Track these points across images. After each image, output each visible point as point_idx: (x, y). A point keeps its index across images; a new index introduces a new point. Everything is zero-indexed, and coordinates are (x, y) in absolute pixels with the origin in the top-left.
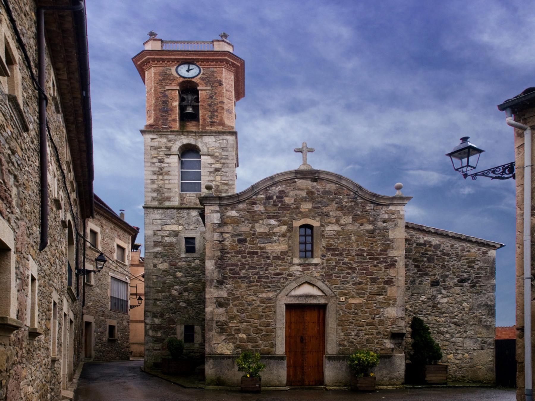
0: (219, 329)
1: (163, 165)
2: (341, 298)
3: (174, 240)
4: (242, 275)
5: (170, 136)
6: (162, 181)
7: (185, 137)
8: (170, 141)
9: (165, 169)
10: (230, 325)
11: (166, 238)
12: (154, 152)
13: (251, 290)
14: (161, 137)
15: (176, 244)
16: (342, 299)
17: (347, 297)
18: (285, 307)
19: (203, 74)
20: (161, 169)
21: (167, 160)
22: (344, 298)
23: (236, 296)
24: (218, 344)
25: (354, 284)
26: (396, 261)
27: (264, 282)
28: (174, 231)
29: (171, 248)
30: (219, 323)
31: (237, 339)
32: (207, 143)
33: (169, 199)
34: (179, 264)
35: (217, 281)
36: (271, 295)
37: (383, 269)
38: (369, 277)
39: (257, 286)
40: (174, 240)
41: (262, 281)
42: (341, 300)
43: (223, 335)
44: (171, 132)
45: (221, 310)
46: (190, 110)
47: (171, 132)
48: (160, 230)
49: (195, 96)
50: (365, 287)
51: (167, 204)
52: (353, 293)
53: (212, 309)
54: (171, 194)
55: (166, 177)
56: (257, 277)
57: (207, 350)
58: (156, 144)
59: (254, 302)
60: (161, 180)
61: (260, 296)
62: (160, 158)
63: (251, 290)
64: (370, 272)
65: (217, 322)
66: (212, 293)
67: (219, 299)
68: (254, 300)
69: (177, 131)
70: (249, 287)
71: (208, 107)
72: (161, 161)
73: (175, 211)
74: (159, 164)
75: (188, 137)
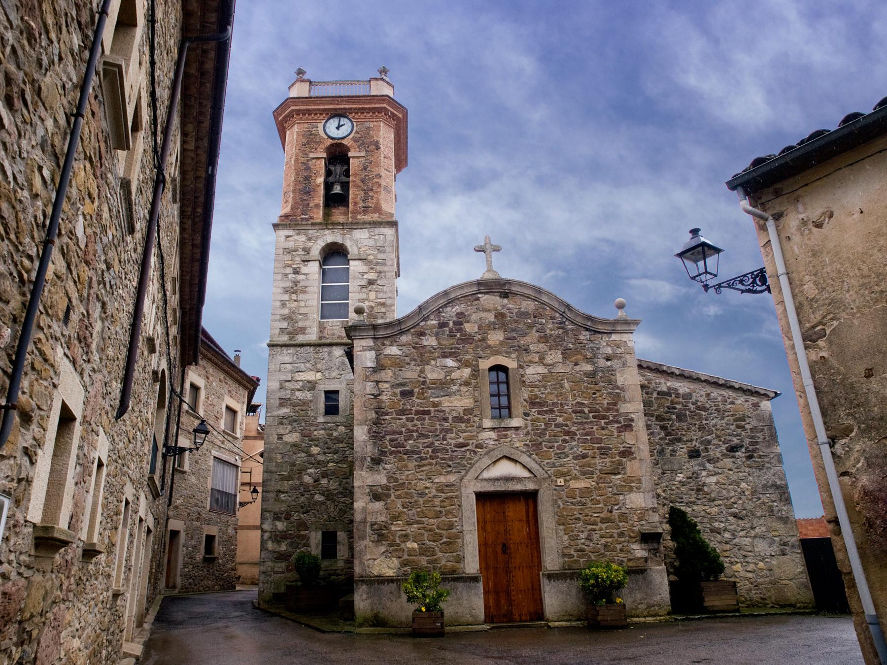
0: (376, 536)
2: (559, 480)
3: (308, 395)
11: (298, 393)
15: (311, 401)
16: (560, 481)
17: (568, 478)
22: (562, 480)
23: (400, 481)
25: (575, 458)
26: (632, 420)
28: (309, 382)
29: (304, 408)
37: (616, 433)
38: (596, 445)
40: (308, 395)
42: (559, 484)
43: (382, 545)
45: (379, 505)
52: (575, 472)
59: (427, 491)
61: (437, 480)
64: (597, 438)
66: (363, 479)
67: (374, 488)
68: (427, 488)
70: (419, 466)
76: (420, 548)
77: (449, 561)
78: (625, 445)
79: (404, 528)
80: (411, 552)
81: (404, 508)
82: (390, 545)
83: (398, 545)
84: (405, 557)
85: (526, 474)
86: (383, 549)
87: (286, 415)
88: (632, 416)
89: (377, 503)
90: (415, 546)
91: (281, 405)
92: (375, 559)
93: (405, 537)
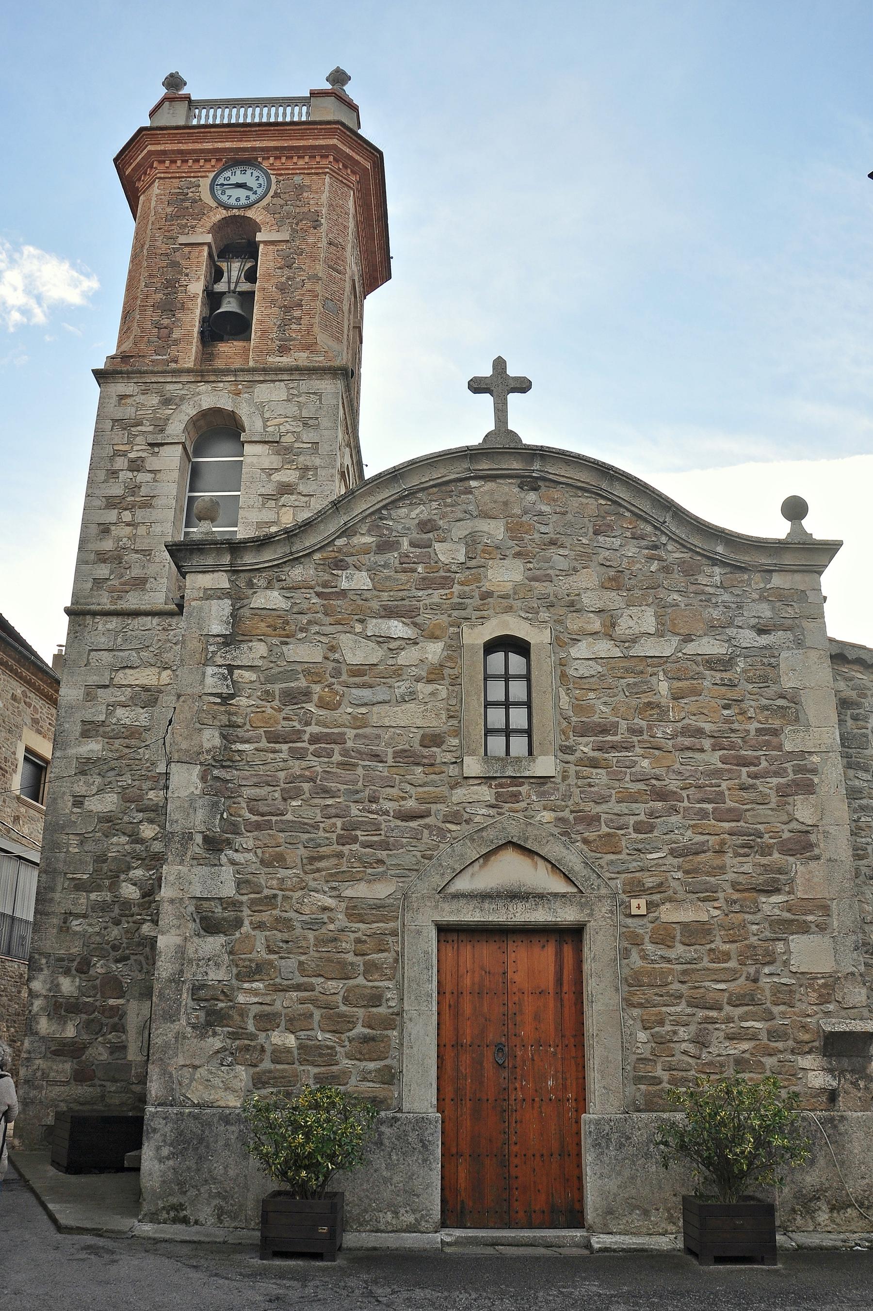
0: (202, 1014)
1: (141, 477)
2: (634, 903)
3: (140, 716)
4: (289, 817)
5: (169, 387)
6: (129, 529)
7: (209, 387)
8: (166, 402)
9: (144, 491)
10: (241, 999)
11: (120, 712)
12: (119, 437)
13: (318, 870)
14: (144, 392)
15: (147, 729)
16: (638, 905)
17: (656, 897)
18: (434, 934)
19: (276, 195)
20: (134, 489)
21: (153, 463)
22: (642, 902)
23: (266, 892)
24: (195, 1067)
25: (672, 853)
26: (814, 771)
27: (366, 845)
28: (146, 689)
29: (133, 742)
30: (202, 993)
31: (263, 1049)
32: (264, 407)
33: (140, 583)
34: (151, 794)
35: (206, 839)
36: (382, 891)
37: (774, 799)
38: (726, 825)
39: (340, 855)
40: (140, 716)
41: (355, 840)
42: (634, 911)
43: (215, 1034)
44: (174, 372)
45: (214, 944)
46: (229, 306)
47: (174, 372)
48: (106, 687)
49: (248, 265)
50: (717, 862)
51: (132, 601)
52: (674, 884)
53: (178, 940)
54: (151, 570)
55: (140, 514)
56: (339, 823)
57: (155, 1088)
58: (128, 412)
59: (325, 917)
60: (128, 524)
61: (349, 893)
62: (132, 455)
63: (318, 870)
64: (730, 810)
65: (196, 989)
66: (185, 880)
67: (206, 904)
68: (325, 909)
69: (189, 371)
70: (312, 859)
71: (277, 295)
72: (136, 466)
73: (156, 620)
74: (130, 475)
75: (214, 389)
76: (301, 1047)
77: (364, 1079)
78: (794, 825)
79: (268, 999)
80: (280, 1055)
81: (271, 951)
82: (234, 1036)
83: (252, 1037)
84: (267, 1064)
85: (559, 886)
86: (216, 1043)
87: (94, 756)
88: (815, 759)
89: (210, 939)
90: (291, 1041)
91: (85, 735)
92: (195, 1067)
93: (267, 1021)
